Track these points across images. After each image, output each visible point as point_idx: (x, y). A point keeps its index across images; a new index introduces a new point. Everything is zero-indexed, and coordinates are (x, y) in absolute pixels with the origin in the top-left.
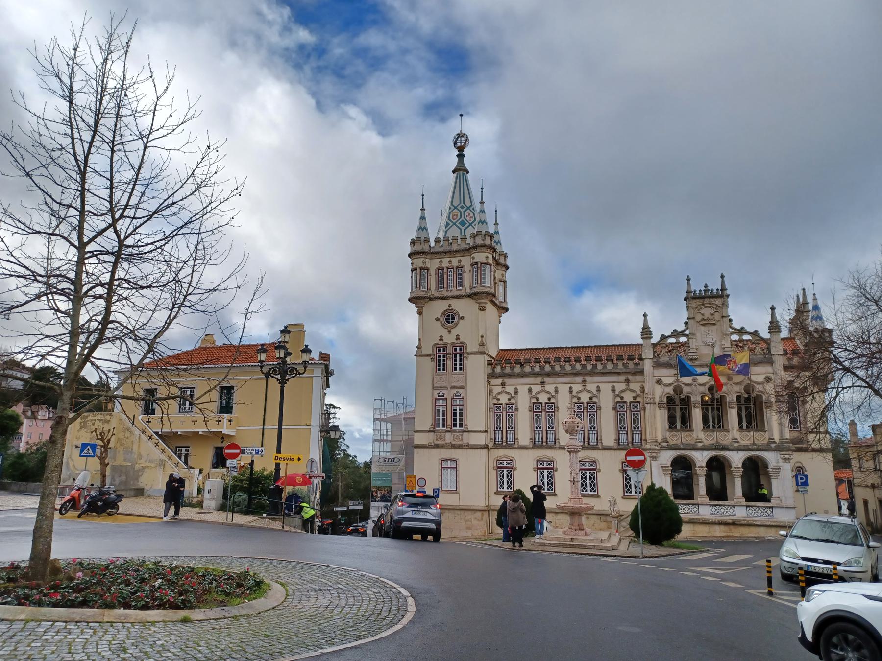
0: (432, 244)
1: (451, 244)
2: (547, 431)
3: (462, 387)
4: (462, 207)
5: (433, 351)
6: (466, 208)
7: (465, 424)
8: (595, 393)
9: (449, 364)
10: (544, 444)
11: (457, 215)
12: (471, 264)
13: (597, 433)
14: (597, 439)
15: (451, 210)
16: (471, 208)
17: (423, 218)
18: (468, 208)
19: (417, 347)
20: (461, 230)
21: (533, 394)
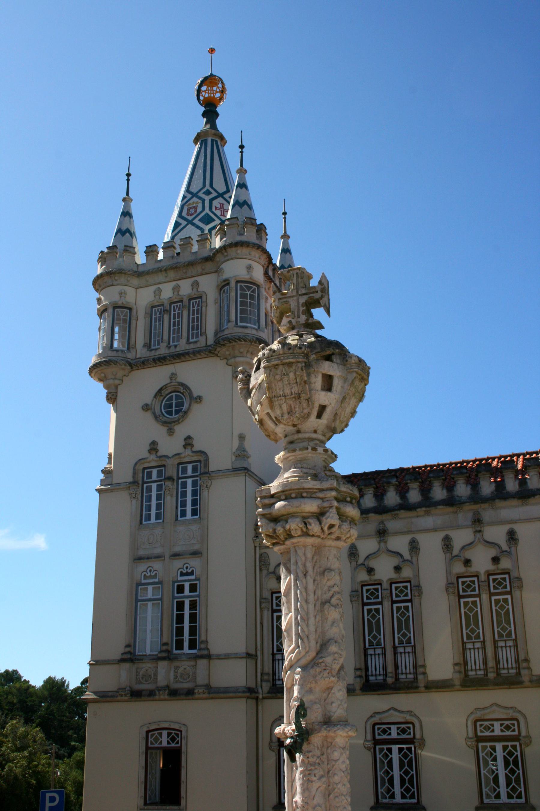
0: (140, 258)
1: (178, 254)
2: (395, 648)
3: (196, 554)
4: (208, 193)
5: (134, 477)
6: (214, 194)
7: (203, 638)
8: (505, 547)
9: (170, 502)
10: (390, 680)
11: (196, 208)
12: (218, 286)
13: (516, 646)
14: (517, 660)
15: (185, 201)
16: (226, 196)
17: (126, 214)
18: (221, 195)
19: (104, 471)
20: (202, 230)
21: (361, 561)
